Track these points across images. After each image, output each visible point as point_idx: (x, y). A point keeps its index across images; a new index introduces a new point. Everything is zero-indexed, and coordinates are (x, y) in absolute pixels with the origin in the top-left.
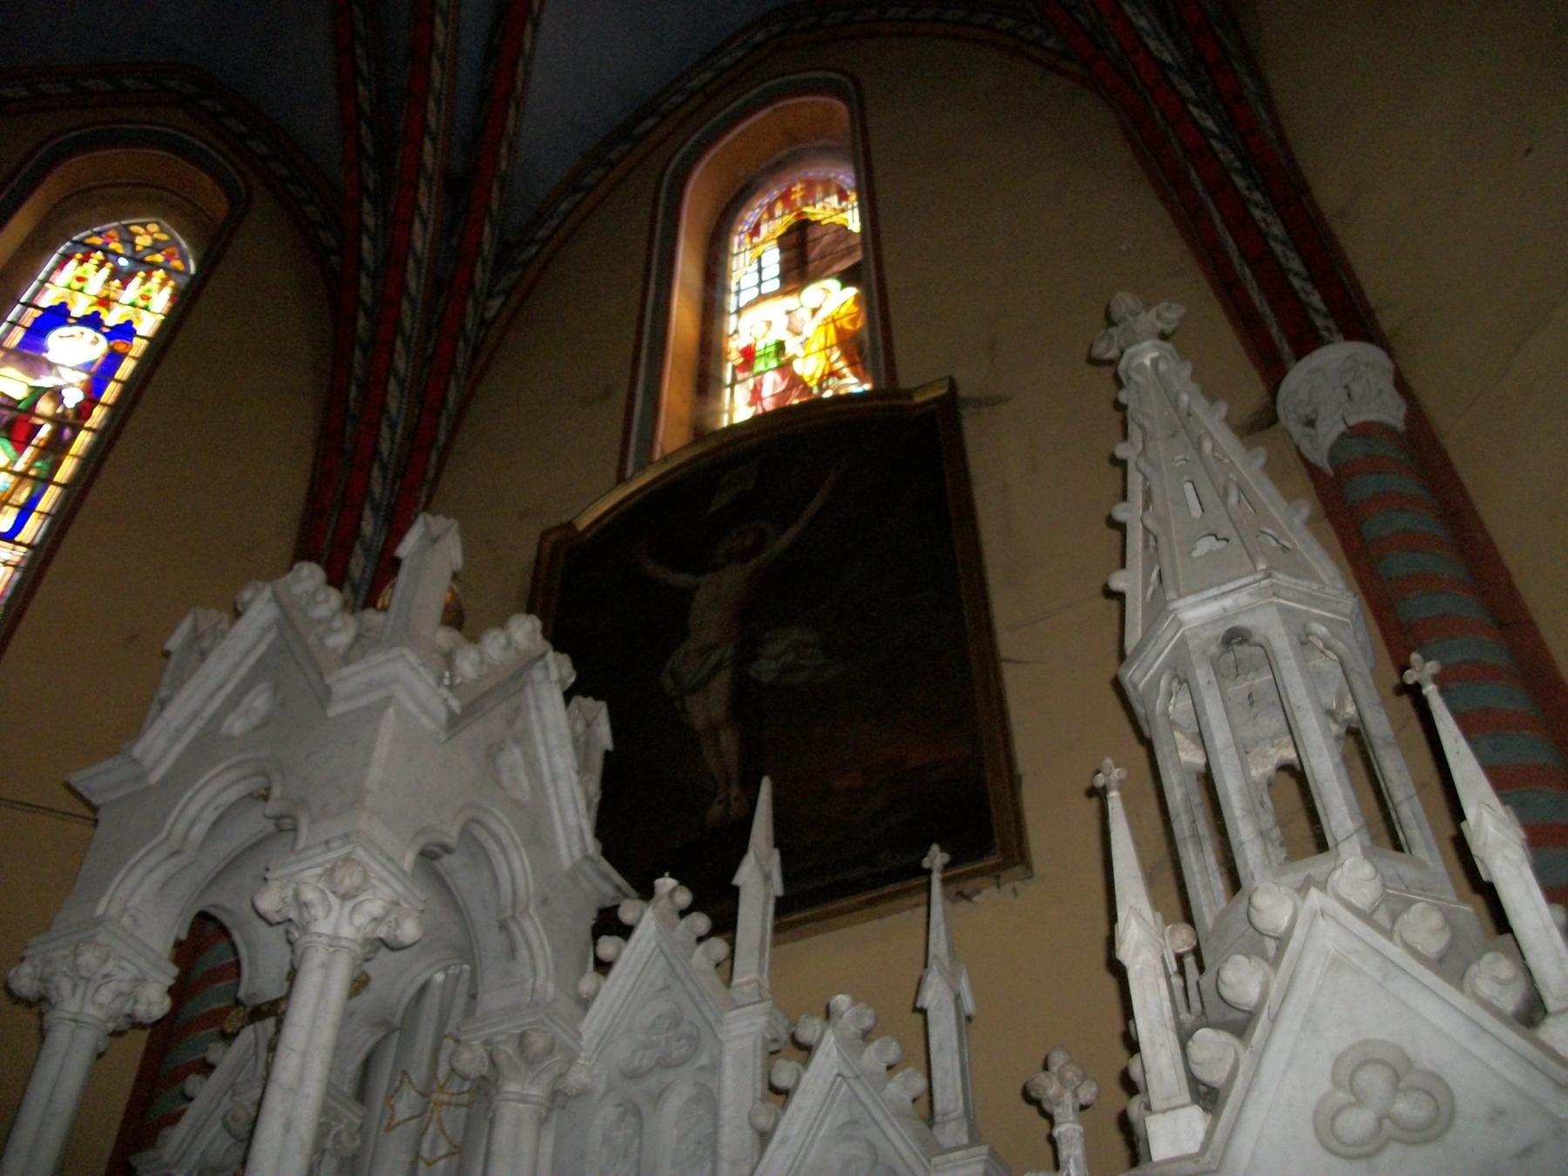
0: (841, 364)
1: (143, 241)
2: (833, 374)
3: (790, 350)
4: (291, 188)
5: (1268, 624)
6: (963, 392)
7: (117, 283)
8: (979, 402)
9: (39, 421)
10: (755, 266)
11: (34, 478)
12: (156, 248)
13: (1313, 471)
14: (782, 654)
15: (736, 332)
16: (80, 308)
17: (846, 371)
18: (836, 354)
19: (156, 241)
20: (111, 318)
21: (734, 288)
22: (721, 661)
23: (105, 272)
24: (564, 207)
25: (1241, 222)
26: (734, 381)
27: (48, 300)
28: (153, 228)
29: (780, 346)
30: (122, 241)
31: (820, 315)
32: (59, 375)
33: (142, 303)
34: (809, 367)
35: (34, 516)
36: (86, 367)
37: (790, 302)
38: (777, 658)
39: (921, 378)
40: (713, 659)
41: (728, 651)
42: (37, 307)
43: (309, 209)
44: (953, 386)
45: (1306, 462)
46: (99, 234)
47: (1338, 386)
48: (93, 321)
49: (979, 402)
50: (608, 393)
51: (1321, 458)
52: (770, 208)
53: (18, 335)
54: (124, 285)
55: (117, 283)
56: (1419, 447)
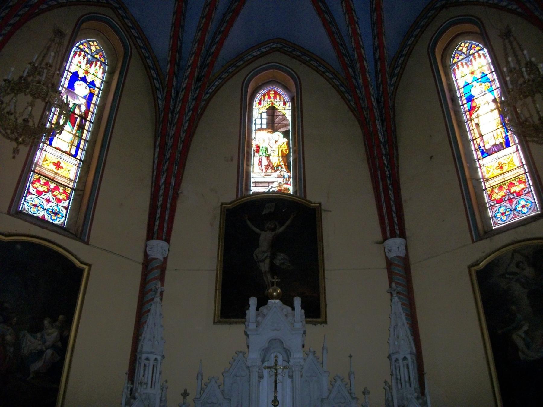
0: (282, 163)
1: (93, 48)
2: (280, 165)
3: (269, 152)
4: (143, 51)
5: (408, 356)
6: (322, 207)
7: (88, 65)
8: (325, 211)
9: (77, 116)
10: (260, 117)
11: (78, 136)
12: (97, 52)
13: (386, 257)
14: (281, 258)
15: (255, 138)
16: (81, 75)
17: (283, 166)
18: (281, 159)
19: (96, 49)
20: (89, 79)
21: (254, 122)
22: (266, 257)
23: (85, 60)
24: (217, 83)
25: (387, 195)
26: (254, 156)
27: (73, 70)
28: (95, 43)
29: (267, 150)
30: (88, 48)
31: (277, 143)
32: (79, 100)
33: (96, 74)
34: (275, 160)
35: (80, 150)
36: (85, 97)
37: (269, 135)
38: (280, 260)
39: (313, 197)
40: (266, 255)
41: (268, 254)
42: (70, 72)
43: (148, 61)
44: (320, 204)
45: (386, 255)
46: (82, 44)
47: (395, 245)
48: (84, 79)
49: (325, 211)
50: (232, 160)
51: (389, 258)
52: (264, 96)
53: (67, 82)
54: (91, 65)
55: (88, 65)
56: (405, 261)
